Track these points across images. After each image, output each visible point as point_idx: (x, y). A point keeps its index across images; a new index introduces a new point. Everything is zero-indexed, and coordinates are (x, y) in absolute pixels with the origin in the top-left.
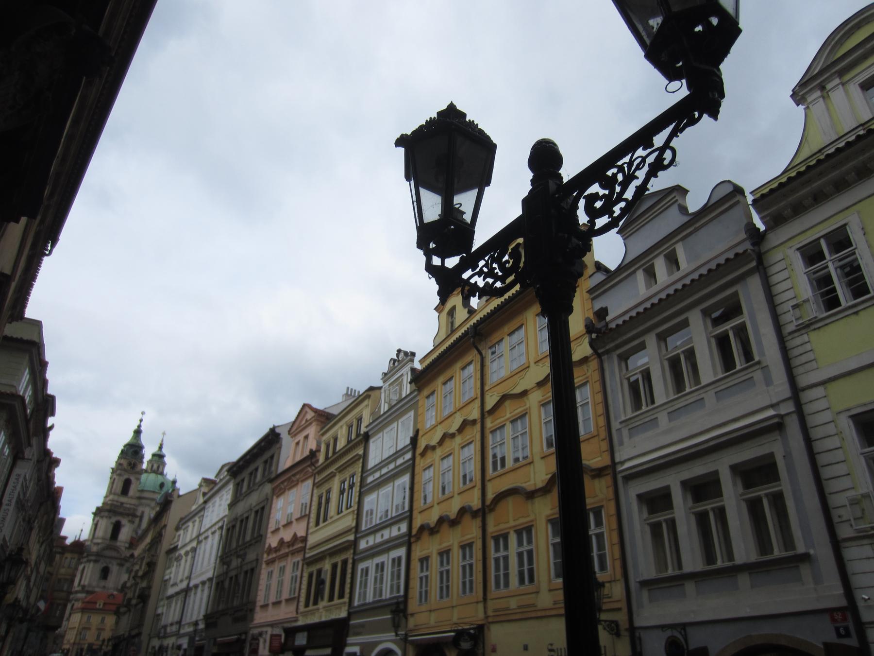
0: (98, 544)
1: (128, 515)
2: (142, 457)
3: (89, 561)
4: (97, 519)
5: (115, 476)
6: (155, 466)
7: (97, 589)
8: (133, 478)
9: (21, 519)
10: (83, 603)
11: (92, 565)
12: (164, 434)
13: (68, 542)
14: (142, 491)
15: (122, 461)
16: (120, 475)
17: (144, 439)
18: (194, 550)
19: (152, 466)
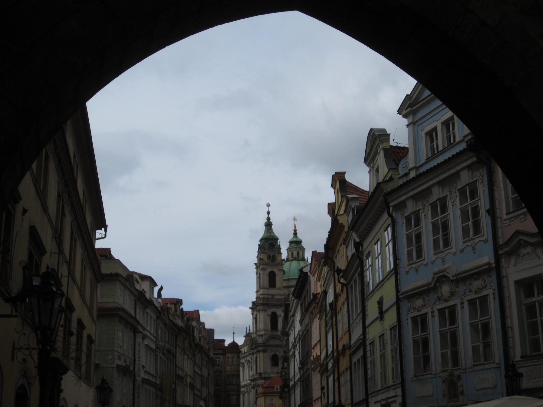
0: (262, 336)
1: (281, 305)
2: (279, 248)
3: (259, 352)
4: (255, 313)
5: (259, 272)
6: (295, 253)
7: (272, 375)
8: (275, 270)
9: (160, 355)
10: (263, 388)
11: (261, 354)
12: (295, 219)
13: (226, 344)
14: (289, 280)
15: (262, 256)
16: (263, 269)
17: (276, 230)
18: (294, 353)
19: (292, 253)
